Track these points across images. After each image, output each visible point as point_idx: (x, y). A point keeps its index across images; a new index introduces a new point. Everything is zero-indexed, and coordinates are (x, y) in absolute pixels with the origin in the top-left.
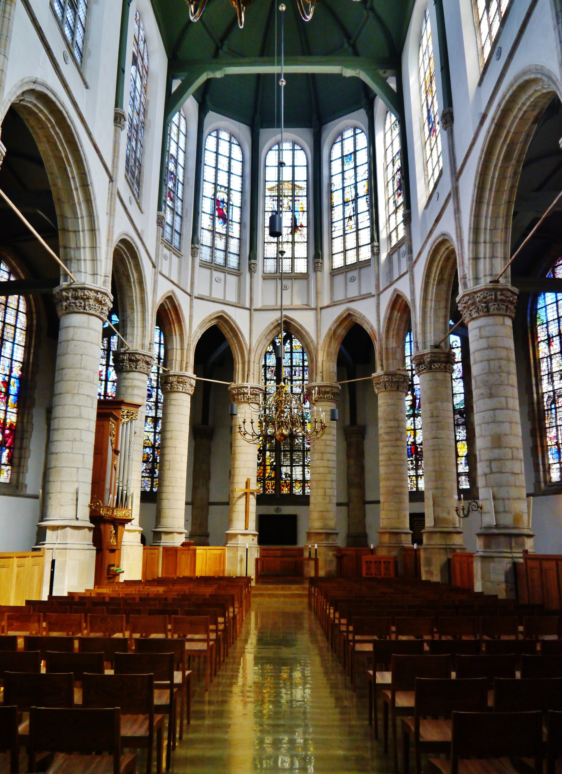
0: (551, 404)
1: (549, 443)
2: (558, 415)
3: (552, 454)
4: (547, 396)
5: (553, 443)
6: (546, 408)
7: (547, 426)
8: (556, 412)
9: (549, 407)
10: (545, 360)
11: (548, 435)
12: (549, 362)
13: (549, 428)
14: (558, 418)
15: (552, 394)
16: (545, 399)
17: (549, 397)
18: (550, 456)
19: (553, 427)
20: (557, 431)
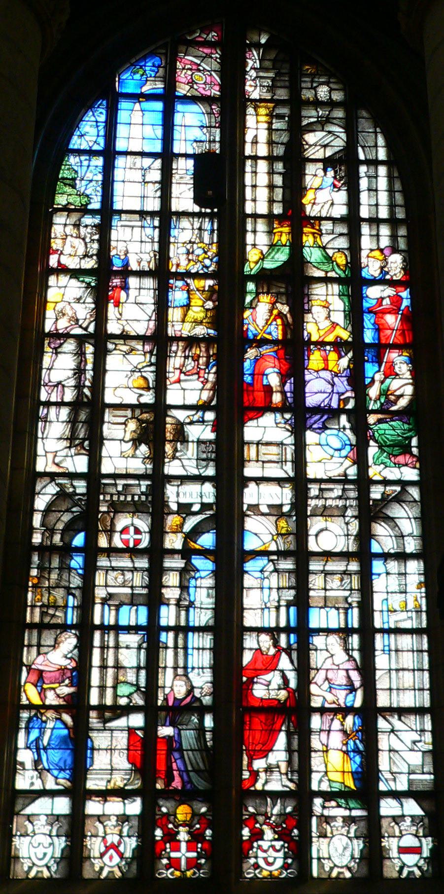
0: (70, 529)
1: (31, 694)
2: (100, 578)
3: (37, 747)
4: (52, 489)
5: (51, 699)
6: (37, 539)
7: (33, 616)
8: (90, 569)
9: (57, 538)
10: (70, 346)
11: (29, 656)
12: (90, 358)
13: (41, 627)
14: (100, 593)
15: (81, 486)
16: (41, 503)
17: (62, 495)
18: (25, 756)
19: (64, 627)
20: (84, 648)
